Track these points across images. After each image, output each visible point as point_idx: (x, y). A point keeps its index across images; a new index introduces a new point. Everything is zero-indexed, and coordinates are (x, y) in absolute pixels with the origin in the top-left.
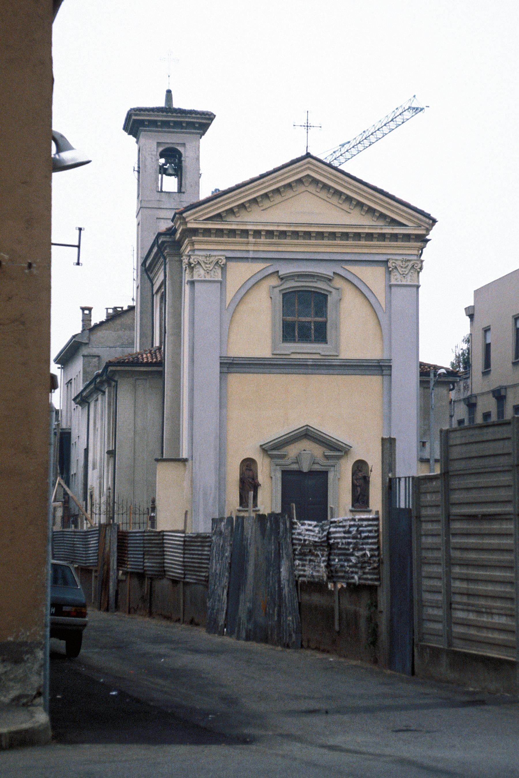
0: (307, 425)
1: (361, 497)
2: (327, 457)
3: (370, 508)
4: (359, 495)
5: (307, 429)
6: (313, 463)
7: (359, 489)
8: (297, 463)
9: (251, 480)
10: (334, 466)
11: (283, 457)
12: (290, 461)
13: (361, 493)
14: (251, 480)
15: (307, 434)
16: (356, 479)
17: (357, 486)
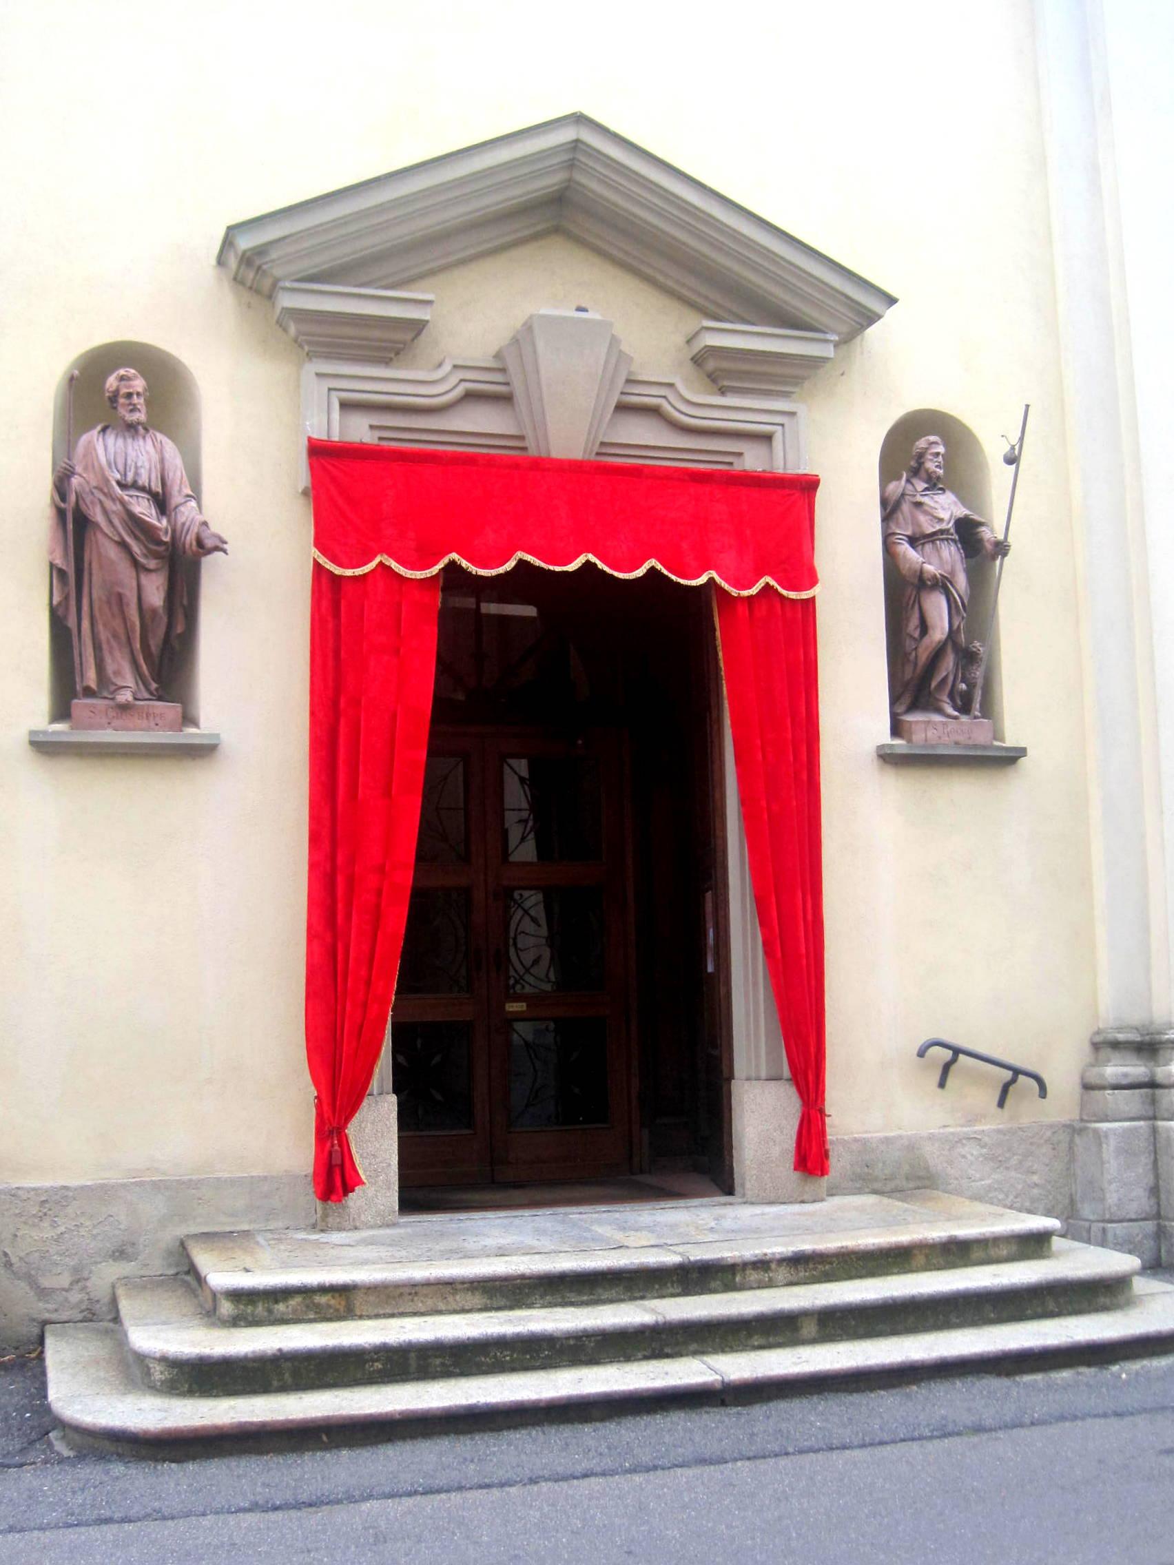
0: (579, 119)
1: (949, 663)
2: (718, 370)
3: (1012, 738)
4: (937, 655)
5: (576, 144)
6: (622, 408)
7: (937, 609)
8: (504, 399)
9: (143, 508)
10: (767, 438)
11: (394, 341)
12: (447, 388)
13: (953, 633)
14: (143, 508)
15: (574, 198)
16: (913, 541)
17: (925, 583)
